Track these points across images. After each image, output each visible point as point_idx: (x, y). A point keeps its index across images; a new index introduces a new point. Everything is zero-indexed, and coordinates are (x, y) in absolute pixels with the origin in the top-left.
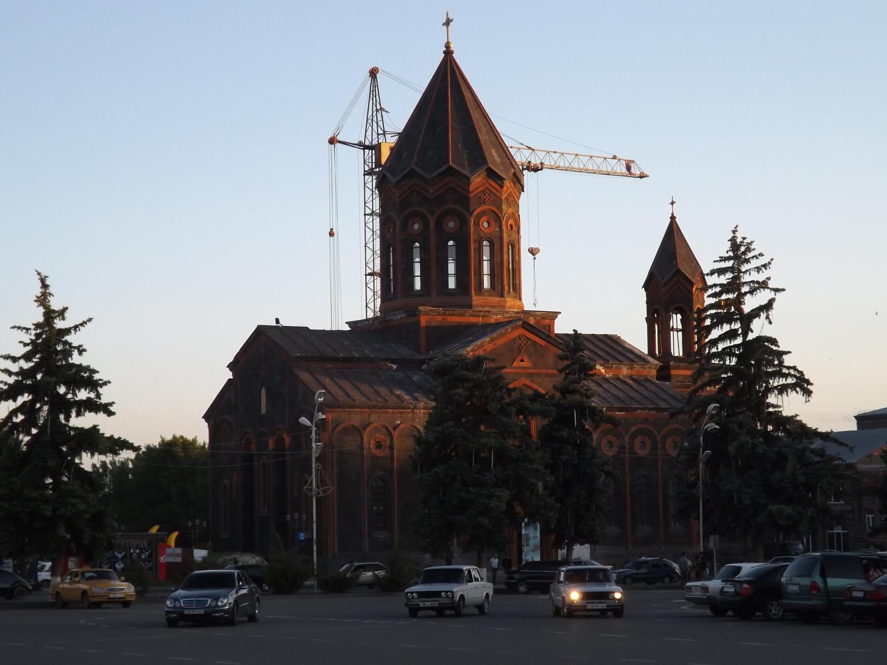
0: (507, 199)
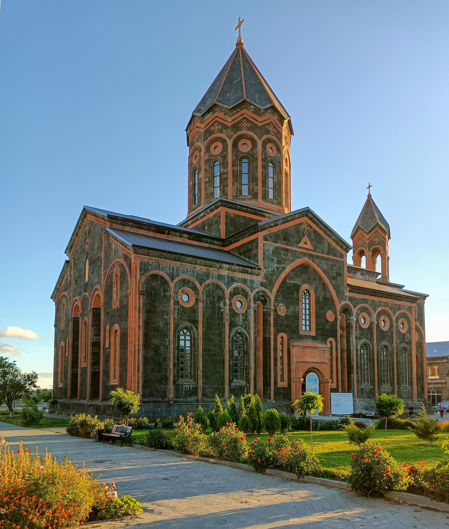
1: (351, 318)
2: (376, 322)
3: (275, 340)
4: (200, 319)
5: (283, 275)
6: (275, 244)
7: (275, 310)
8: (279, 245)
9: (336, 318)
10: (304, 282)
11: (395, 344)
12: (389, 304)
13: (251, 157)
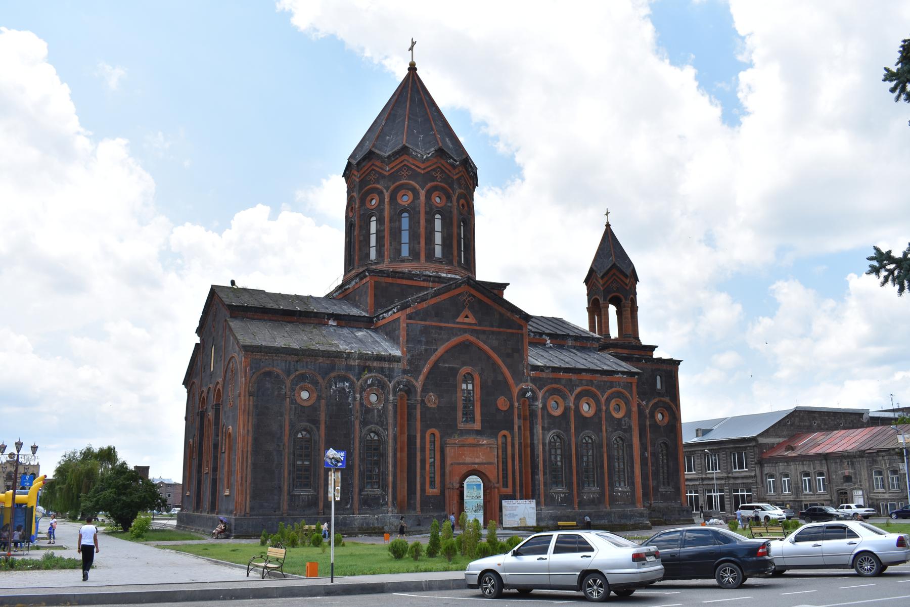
0: (458, 179)
1: (536, 404)
2: (573, 407)
3: (423, 438)
4: (323, 417)
5: (433, 358)
6: (423, 323)
7: (423, 401)
8: (427, 323)
9: (512, 406)
10: (464, 364)
11: (604, 434)
13: (412, 210)
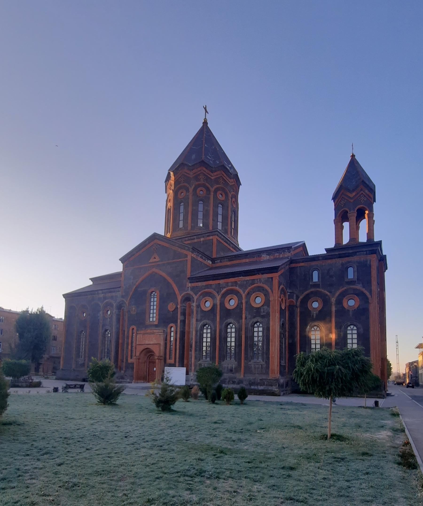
9: (177, 308)
11: (243, 320)
12: (238, 282)
